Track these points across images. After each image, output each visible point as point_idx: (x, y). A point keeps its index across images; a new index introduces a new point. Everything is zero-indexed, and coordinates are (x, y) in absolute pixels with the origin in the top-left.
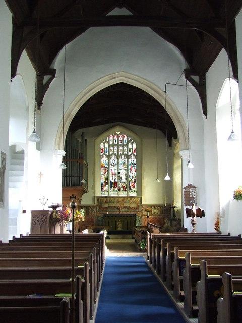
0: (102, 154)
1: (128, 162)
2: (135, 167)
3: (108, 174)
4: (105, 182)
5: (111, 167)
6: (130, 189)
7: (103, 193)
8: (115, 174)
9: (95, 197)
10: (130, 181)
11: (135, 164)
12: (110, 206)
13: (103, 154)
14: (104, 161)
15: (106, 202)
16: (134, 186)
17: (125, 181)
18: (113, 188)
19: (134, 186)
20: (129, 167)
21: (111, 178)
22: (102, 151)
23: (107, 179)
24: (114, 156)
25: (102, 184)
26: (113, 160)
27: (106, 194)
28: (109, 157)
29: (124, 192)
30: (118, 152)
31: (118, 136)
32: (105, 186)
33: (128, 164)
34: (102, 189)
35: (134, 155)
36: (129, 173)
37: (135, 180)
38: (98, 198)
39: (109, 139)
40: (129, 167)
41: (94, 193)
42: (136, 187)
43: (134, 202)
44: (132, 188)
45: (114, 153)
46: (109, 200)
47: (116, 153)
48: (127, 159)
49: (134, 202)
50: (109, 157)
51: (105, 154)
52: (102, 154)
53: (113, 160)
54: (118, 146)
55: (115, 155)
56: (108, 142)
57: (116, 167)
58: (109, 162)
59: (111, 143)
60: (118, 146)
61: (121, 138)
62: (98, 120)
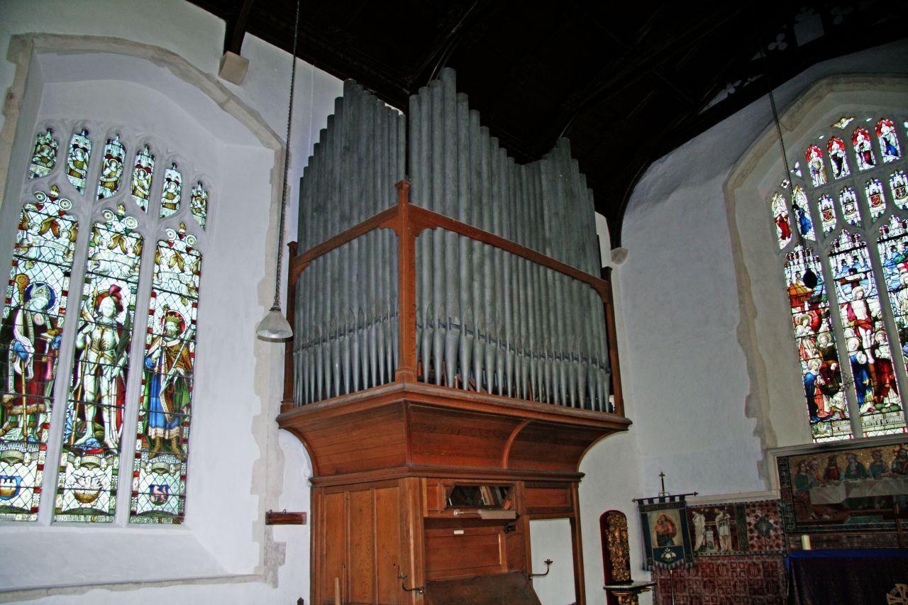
0: (783, 244)
4: (825, 371)
7: (822, 427)
8: (870, 322)
9: (765, 451)
12: (855, 494)
15: (831, 475)
18: (869, 394)
21: (852, 343)
22: (782, 223)
23: (830, 355)
25: (810, 385)
27: (842, 433)
30: (863, 209)
31: (848, 140)
34: (813, 408)
39: (804, 168)
45: (842, 224)
46: (842, 462)
47: (854, 217)
52: (783, 244)
54: (857, 182)
55: (852, 229)
56: (805, 183)
57: (868, 285)
59: (819, 180)
60: (857, 182)
61: (863, 142)
62: (722, 96)
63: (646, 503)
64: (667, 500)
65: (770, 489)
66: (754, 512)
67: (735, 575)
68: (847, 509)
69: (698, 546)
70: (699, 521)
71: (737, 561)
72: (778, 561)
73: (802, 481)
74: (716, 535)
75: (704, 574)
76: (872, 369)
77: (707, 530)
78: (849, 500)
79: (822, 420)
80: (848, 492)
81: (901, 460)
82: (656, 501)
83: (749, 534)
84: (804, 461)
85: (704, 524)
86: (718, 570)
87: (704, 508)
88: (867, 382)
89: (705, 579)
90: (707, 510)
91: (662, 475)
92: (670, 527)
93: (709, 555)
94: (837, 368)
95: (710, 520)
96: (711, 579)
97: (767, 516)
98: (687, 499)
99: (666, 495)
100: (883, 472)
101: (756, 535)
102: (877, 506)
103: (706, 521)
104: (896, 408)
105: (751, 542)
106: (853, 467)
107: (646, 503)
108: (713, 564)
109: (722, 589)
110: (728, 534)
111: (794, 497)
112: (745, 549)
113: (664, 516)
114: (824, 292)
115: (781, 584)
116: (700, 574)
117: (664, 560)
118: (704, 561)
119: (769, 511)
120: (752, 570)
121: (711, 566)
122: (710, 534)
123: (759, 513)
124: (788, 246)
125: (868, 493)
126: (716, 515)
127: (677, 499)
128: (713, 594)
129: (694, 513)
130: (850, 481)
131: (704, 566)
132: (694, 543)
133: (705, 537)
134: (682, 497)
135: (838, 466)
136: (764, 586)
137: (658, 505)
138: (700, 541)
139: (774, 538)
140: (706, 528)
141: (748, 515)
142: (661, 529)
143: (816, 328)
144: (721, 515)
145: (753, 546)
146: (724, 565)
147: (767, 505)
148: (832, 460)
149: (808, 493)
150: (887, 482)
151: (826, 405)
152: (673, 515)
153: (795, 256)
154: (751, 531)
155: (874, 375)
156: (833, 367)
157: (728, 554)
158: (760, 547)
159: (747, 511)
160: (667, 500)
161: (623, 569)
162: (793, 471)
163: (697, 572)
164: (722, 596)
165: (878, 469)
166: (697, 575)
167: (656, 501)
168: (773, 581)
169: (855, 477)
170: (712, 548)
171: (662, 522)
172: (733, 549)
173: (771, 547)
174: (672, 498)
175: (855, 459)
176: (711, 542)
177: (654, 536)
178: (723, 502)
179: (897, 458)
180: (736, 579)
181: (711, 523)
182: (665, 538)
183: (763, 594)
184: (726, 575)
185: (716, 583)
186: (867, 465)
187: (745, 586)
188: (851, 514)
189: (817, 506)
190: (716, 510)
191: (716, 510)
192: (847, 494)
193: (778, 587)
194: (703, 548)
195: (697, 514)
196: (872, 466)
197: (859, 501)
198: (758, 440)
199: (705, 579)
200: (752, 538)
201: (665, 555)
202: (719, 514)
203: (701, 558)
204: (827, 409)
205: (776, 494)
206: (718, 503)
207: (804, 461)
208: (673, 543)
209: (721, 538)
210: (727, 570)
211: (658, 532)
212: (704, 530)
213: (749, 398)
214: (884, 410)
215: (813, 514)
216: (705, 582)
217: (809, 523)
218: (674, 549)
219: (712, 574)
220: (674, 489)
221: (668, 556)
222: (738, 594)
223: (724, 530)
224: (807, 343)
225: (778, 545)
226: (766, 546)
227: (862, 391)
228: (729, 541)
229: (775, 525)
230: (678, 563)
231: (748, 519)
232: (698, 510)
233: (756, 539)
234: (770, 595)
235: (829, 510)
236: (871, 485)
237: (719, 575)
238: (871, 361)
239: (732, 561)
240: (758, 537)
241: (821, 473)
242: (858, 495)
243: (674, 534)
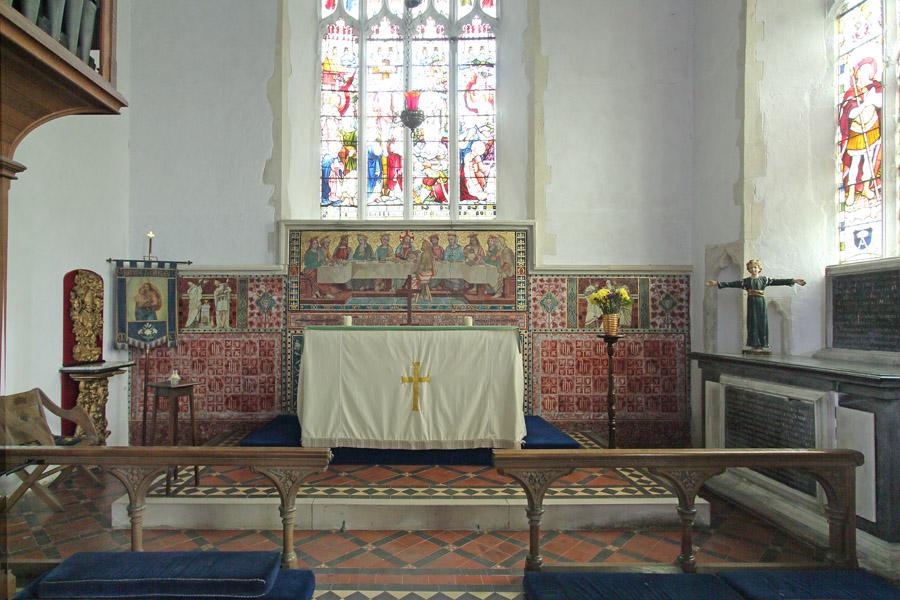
0: (326, 13)
1: (454, 51)
2: (492, 81)
3: (358, 116)
4: (343, 156)
5: (372, 82)
6: (465, 195)
9: (278, 224)
10: (462, 154)
11: (491, 65)
12: (360, 275)
13: (331, 11)
14: (337, 51)
15: (341, 254)
16: (482, 180)
17: (442, 150)
18: (379, 186)
19: (482, 180)
20: (462, 82)
24: (385, 24)
26: (383, 48)
27: (351, 215)
28: (361, 29)
29: (435, 208)
32: (342, 175)
33: (453, 66)
34: (326, 191)
35: (485, 18)
36: (461, 109)
37: (489, 146)
38: (298, 233)
40: (462, 84)
41: (276, 201)
42: (491, 186)
43: (493, 256)
44: (473, 188)
45: (385, 11)
46: (353, 243)
48: (453, 40)
49: (493, 256)
50: (361, 29)
51: (341, 13)
53: (383, 48)
55: (393, 18)
58: (361, 56)
63: (127, 264)
64: (154, 265)
65: (278, 263)
66: (258, 286)
68: (350, 290)
69: (189, 323)
70: (195, 294)
71: (233, 339)
72: (276, 340)
73: (310, 258)
74: (212, 310)
75: (194, 353)
76: (385, 161)
78: (353, 281)
79: (332, 204)
80: (353, 273)
81: (405, 246)
83: (249, 310)
84: (317, 238)
86: (210, 349)
88: (378, 173)
92: (155, 299)
94: (355, 155)
96: (202, 359)
97: (271, 292)
98: (179, 267)
100: (388, 256)
101: (256, 311)
102: (377, 288)
104: (397, 202)
105: (249, 320)
106: (362, 249)
107: (127, 264)
108: (205, 342)
111: (301, 274)
112: (243, 327)
114: (356, 76)
115: (275, 364)
116: (189, 353)
117: (142, 338)
118: (195, 338)
119: (273, 287)
120: (248, 348)
121: (203, 344)
123: (263, 288)
124: (331, 16)
125: (371, 275)
126: (215, 287)
127: (167, 265)
128: (202, 375)
129: (190, 283)
130: (357, 262)
132: (186, 319)
134: (173, 264)
135: (349, 245)
136: (258, 366)
137: (143, 271)
138: (192, 316)
139: (275, 315)
140: (202, 301)
141: (251, 289)
142: (142, 301)
143: (342, 111)
144: (221, 288)
145: (251, 323)
146: (217, 343)
147: (272, 281)
148: (344, 240)
149: (316, 271)
150: (389, 265)
151: (337, 189)
152: (161, 285)
153: (335, 30)
154: (252, 307)
155: (385, 168)
156: (352, 151)
158: (259, 325)
159: (250, 285)
160: (154, 265)
161: (90, 345)
162: (305, 248)
163: (187, 349)
164: (212, 377)
165: (384, 253)
167: (141, 265)
168: (268, 361)
169: (362, 259)
170: (206, 323)
171: (145, 292)
173: (271, 325)
174: (161, 264)
175: (365, 241)
176: (205, 317)
179: (402, 244)
180: (229, 359)
181: (209, 297)
182: (146, 310)
183: (256, 374)
184: (219, 355)
185: (206, 363)
186: (375, 250)
187: (238, 366)
188: (353, 295)
189: (323, 285)
190: (216, 282)
191: (216, 282)
192: (353, 274)
193: (272, 367)
194: (195, 324)
196: (380, 248)
197: (363, 281)
198: (272, 210)
199: (195, 359)
200: (252, 315)
201: (144, 331)
204: (339, 194)
205: (283, 268)
207: (317, 238)
208: (155, 318)
209: (217, 313)
210: (221, 349)
211: (137, 304)
213: (269, 163)
214: (387, 203)
215: (318, 293)
216: (194, 362)
217: (312, 302)
218: (157, 325)
220: (164, 253)
221: (148, 332)
222: (229, 375)
223: (223, 305)
224: (331, 122)
225: (278, 324)
226: (265, 324)
227: (373, 180)
229: (278, 303)
230: (159, 340)
231: (250, 294)
233: (256, 316)
234: (264, 375)
235: (334, 290)
236: (376, 267)
238: (386, 154)
240: (259, 314)
241: (332, 250)
242: (363, 277)
243: (158, 307)
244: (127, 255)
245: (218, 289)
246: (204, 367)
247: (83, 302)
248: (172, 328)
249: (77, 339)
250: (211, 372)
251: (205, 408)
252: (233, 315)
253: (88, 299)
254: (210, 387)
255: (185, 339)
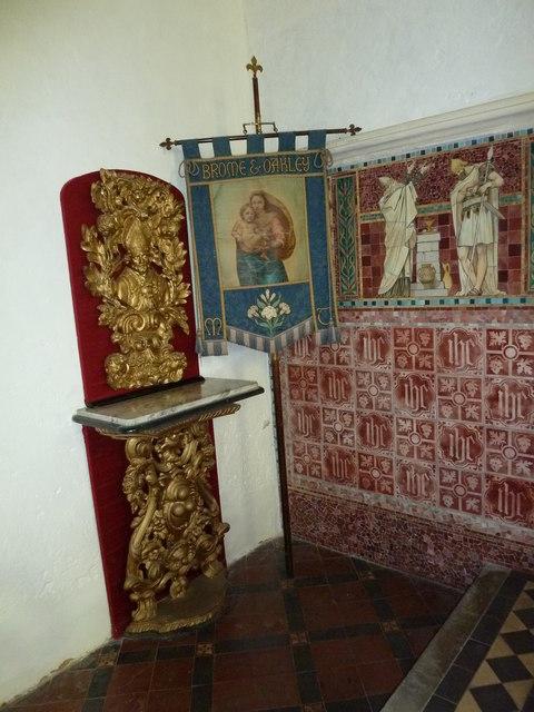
63: (207, 151)
64: (271, 146)
67: (497, 366)
69: (386, 284)
70: (399, 206)
71: (511, 326)
74: (447, 246)
75: (403, 361)
77: (420, 232)
82: (239, 149)
85: (412, 213)
86: (444, 351)
87: (419, 162)
89: (404, 373)
90: (424, 169)
91: (254, 67)
92: (278, 229)
93: (422, 303)
95: (434, 199)
96: (423, 374)
99: (266, 129)
103: (420, 202)
107: (207, 151)
108: (430, 332)
109: (450, 403)
110: (488, 240)
113: (263, 195)
121: (425, 338)
122: (430, 241)
126: (453, 180)
127: (302, 143)
128: (424, 416)
131: (404, 338)
132: (378, 273)
133: (414, 251)
134: (317, 138)
138: (395, 264)
142: (249, 235)
146: (463, 335)
152: (288, 192)
157: (481, 302)
160: (271, 146)
161: (155, 350)
164: (450, 424)
166: (382, 361)
170: (431, 284)
172: (500, 288)
174: (287, 140)
176: (429, 266)
177: (227, 256)
178: (481, 134)
180: (498, 380)
181: (435, 209)
184: (467, 369)
185: (434, 389)
190: (456, 164)
191: (456, 164)
194: (403, 285)
195: (395, 184)
199: (404, 373)
202: (464, 175)
203: (396, 314)
206: (463, 139)
208: (283, 276)
209: (462, 252)
210: (474, 353)
212: (412, 230)
216: (403, 381)
218: (288, 292)
219: (424, 361)
220: (290, 113)
221: (269, 312)
223: (477, 230)
228: (491, 262)
230: (296, 330)
232: (396, 170)
237: (447, 364)
239: (495, 325)
243: (286, 250)
244: (202, 125)
245: (460, 185)
246: (428, 397)
247: (123, 250)
248: (324, 299)
249: (116, 338)
250: (447, 411)
251: (435, 496)
252: (512, 256)
253: (135, 244)
254: (445, 447)
255: (379, 324)
